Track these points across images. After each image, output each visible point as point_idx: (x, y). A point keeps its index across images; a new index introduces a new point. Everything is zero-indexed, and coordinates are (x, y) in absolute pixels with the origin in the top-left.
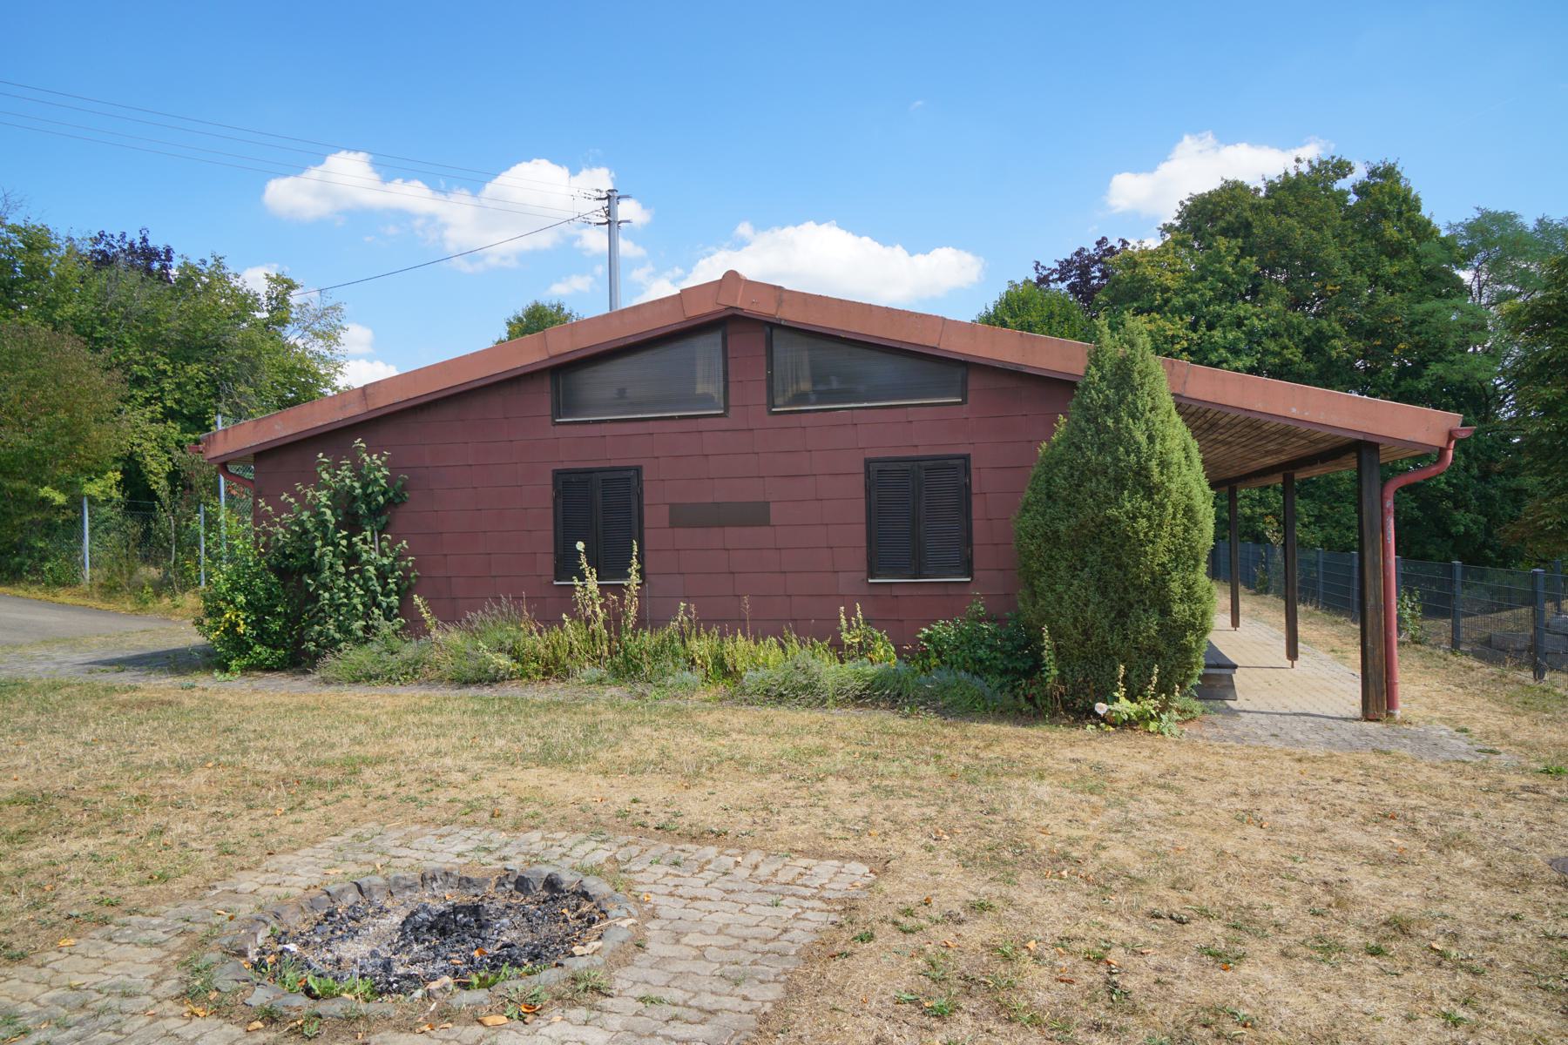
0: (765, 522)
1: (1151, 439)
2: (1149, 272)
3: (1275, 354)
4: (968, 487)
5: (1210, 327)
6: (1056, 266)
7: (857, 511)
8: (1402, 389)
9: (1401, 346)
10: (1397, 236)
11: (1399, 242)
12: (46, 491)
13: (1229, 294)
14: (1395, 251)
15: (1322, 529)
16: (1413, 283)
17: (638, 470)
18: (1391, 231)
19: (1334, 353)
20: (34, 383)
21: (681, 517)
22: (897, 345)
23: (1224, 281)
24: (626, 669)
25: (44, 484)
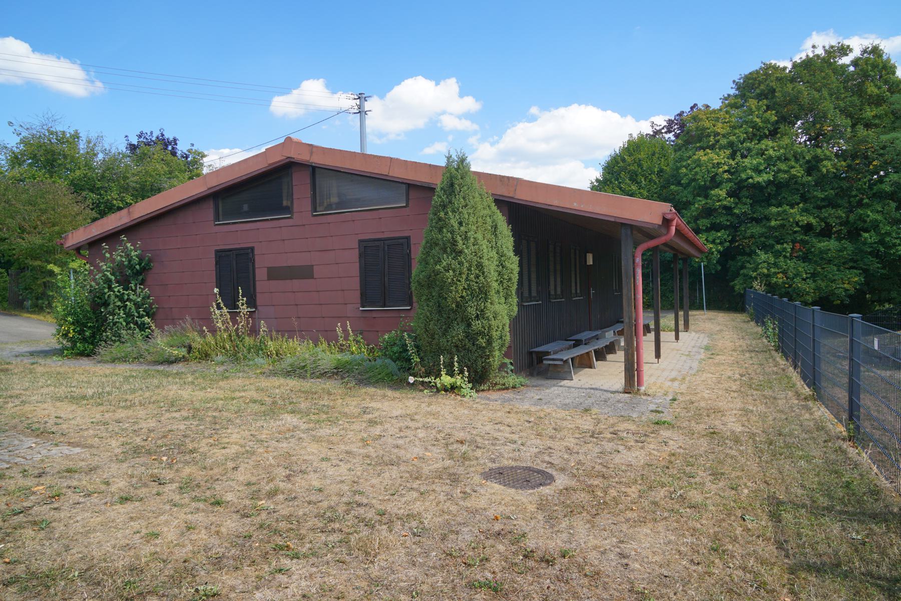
0: (311, 276)
1: (460, 224)
2: (707, 124)
3: (785, 172)
4: (409, 255)
5: (744, 156)
6: (665, 124)
7: (355, 270)
8: (874, 191)
9: (875, 163)
10: (876, 91)
11: (878, 96)
12: (51, 267)
13: (757, 135)
14: (878, 101)
15: (814, 281)
16: (886, 122)
17: (252, 249)
18: (871, 89)
19: (824, 170)
20: (44, 212)
21: (275, 274)
22: (383, 170)
23: (753, 128)
24: (235, 357)
25: (50, 263)
